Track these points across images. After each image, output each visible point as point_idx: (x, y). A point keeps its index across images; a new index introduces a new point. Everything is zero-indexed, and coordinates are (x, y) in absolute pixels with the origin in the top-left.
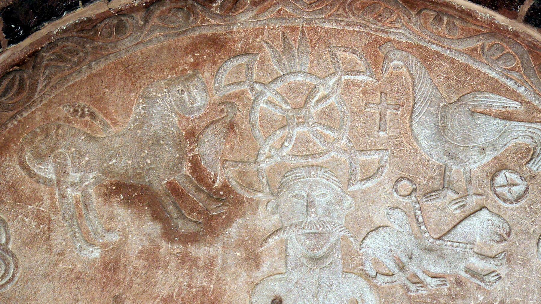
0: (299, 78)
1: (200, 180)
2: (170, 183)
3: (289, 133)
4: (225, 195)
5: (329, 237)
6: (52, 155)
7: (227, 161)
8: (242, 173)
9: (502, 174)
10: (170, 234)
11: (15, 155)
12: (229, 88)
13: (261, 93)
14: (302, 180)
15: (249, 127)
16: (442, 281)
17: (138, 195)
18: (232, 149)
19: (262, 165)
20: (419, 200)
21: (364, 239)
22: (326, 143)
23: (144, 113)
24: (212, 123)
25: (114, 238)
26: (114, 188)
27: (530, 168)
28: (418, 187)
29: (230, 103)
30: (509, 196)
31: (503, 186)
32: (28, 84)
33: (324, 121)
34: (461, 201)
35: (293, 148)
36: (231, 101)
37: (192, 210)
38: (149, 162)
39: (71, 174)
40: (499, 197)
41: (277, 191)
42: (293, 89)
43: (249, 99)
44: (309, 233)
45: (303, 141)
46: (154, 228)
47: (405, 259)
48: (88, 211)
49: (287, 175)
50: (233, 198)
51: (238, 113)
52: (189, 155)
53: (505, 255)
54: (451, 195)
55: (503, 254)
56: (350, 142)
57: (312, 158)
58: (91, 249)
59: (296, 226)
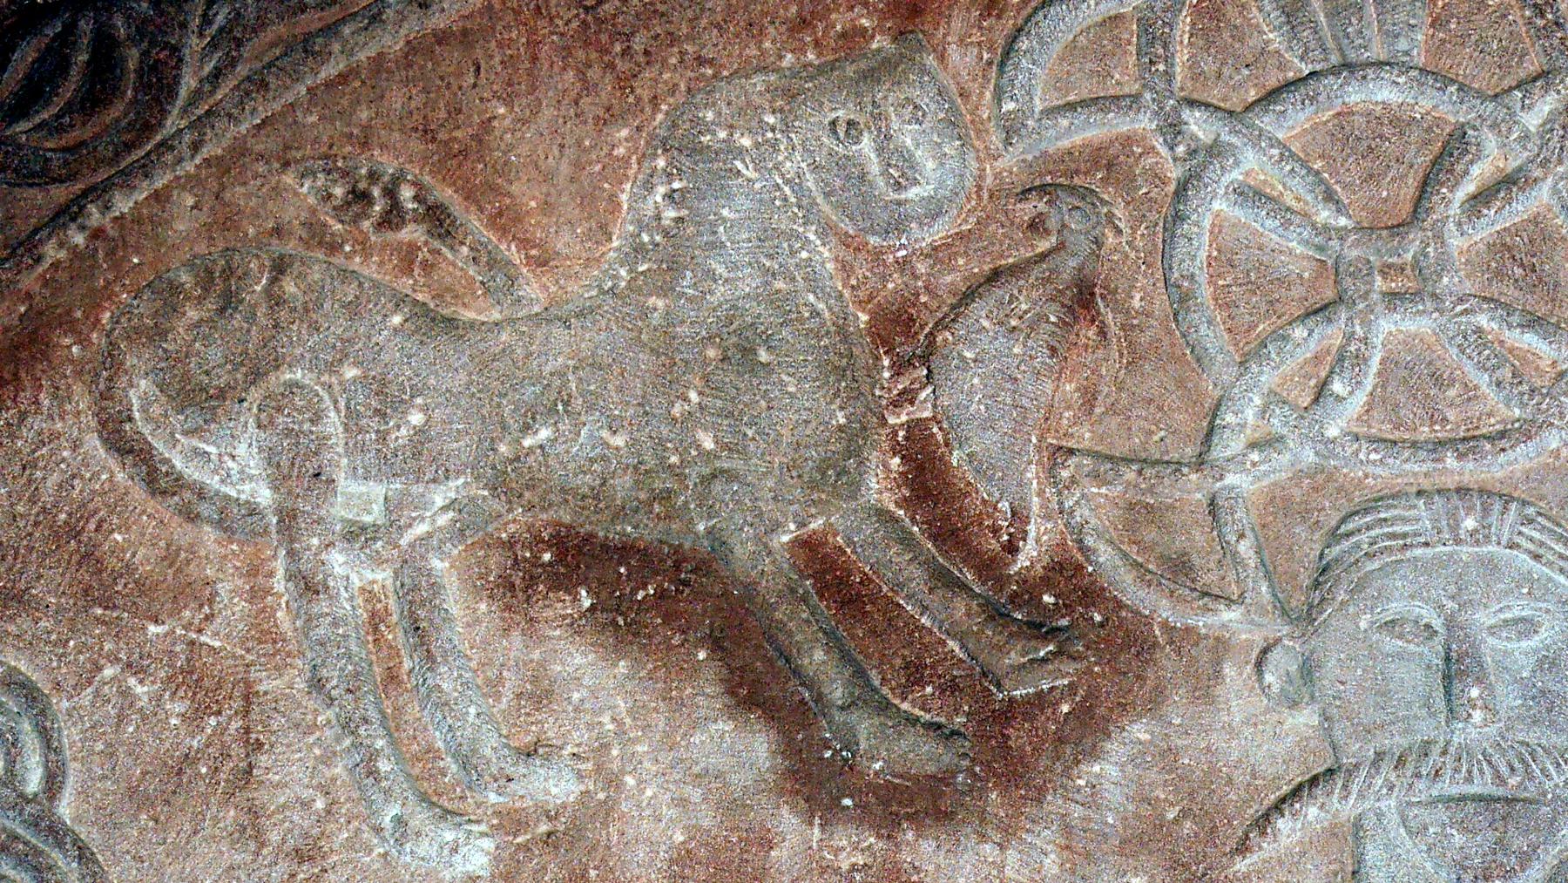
0: (1384, 93)
1: (950, 534)
2: (808, 546)
3: (1350, 337)
4: (1061, 606)
5: (1554, 819)
6: (255, 395)
8: (1139, 515)
10: (816, 780)
11: (78, 388)
12: (1065, 123)
13: (1215, 150)
14: (1419, 552)
15: (1161, 303)
17: (661, 594)
18: (1089, 397)
19: (1230, 479)
22: (1525, 387)
23: (680, 220)
24: (995, 276)
25: (556, 786)
26: (547, 557)
29: (1072, 190)
32: (131, 65)
33: (1510, 292)
35: (1369, 408)
37: (915, 674)
38: (708, 444)
39: (347, 485)
41: (1311, 596)
42: (1358, 140)
43: (1160, 179)
44: (1463, 798)
45: (1413, 377)
48: (430, 656)
49: (1350, 526)
50: (1102, 625)
51: (1111, 239)
57: (1461, 456)
58: (449, 836)
59: (1400, 762)
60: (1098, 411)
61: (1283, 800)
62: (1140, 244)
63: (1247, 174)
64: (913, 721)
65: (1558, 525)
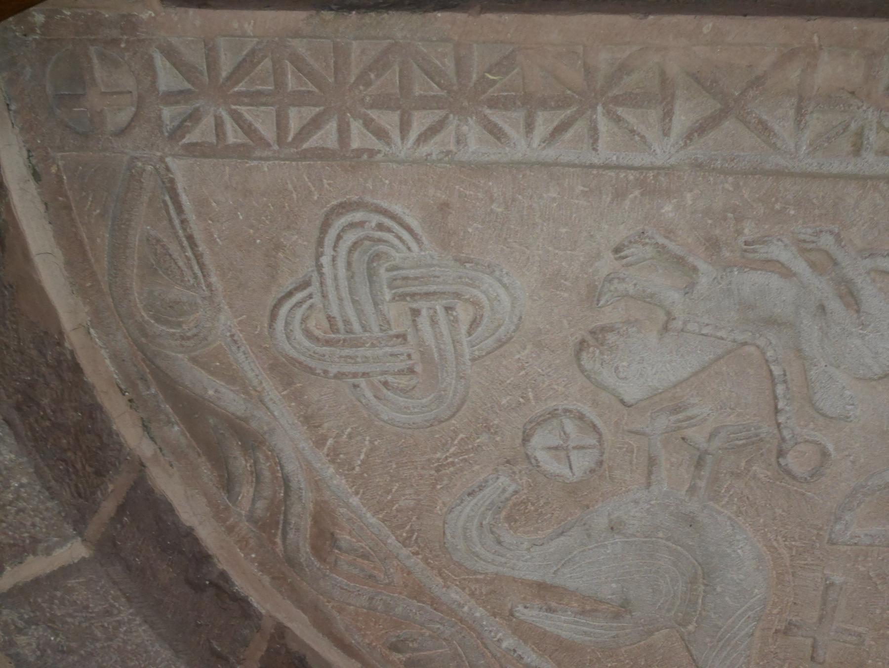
16: (754, 251)
20: (776, 431)
27: (514, 480)
28: (773, 460)
30: (570, 426)
34: (681, 421)
40: (594, 426)
47: (835, 305)
53: (599, 301)
54: (697, 436)
55: (602, 303)
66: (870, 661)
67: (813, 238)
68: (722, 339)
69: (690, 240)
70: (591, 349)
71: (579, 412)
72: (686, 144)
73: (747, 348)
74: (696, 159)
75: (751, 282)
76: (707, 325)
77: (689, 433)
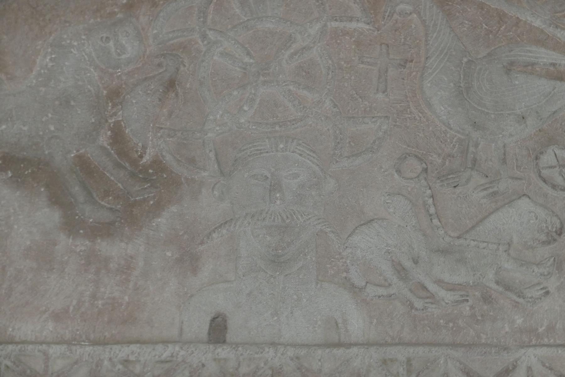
2: (80, 157)
7: (162, 128)
9: (550, 151)
10: (72, 225)
14: (265, 155)
16: (462, 296)
18: (170, 114)
19: (210, 135)
20: (431, 184)
21: (350, 236)
23: (53, 66)
24: (146, 79)
28: (429, 167)
31: (551, 167)
34: (490, 187)
36: (174, 52)
38: (52, 128)
40: (545, 181)
46: (49, 216)
47: (408, 264)
50: (166, 178)
51: (182, 68)
52: (110, 121)
53: (554, 260)
56: (335, 106)
57: (280, 126)
59: (253, 216)
60: (173, 117)
61: (216, 228)
62: (191, 69)
63: (225, 49)
64: (103, 207)
65: (308, 145)
66: (353, 47)
67: (427, 305)
68: (473, 240)
69: (502, 301)
70: (554, 230)
71: (556, 190)
72: (516, 362)
73: (456, 235)
74: (508, 353)
75: (461, 276)
76: (484, 248)
77: (483, 181)
